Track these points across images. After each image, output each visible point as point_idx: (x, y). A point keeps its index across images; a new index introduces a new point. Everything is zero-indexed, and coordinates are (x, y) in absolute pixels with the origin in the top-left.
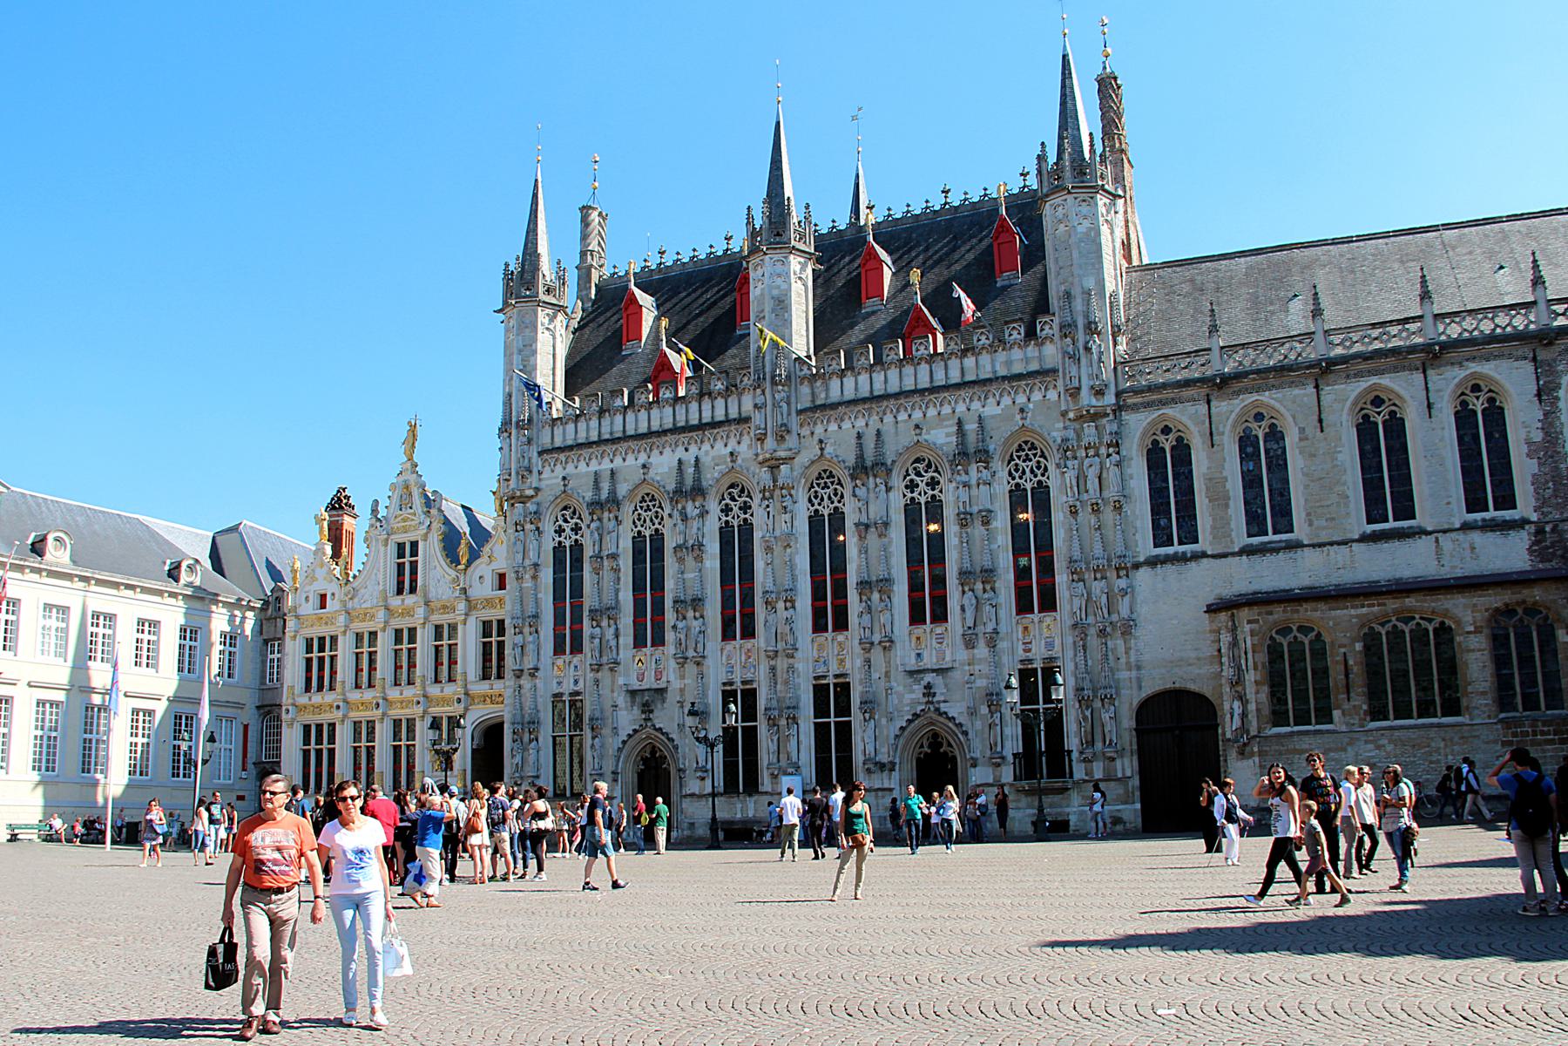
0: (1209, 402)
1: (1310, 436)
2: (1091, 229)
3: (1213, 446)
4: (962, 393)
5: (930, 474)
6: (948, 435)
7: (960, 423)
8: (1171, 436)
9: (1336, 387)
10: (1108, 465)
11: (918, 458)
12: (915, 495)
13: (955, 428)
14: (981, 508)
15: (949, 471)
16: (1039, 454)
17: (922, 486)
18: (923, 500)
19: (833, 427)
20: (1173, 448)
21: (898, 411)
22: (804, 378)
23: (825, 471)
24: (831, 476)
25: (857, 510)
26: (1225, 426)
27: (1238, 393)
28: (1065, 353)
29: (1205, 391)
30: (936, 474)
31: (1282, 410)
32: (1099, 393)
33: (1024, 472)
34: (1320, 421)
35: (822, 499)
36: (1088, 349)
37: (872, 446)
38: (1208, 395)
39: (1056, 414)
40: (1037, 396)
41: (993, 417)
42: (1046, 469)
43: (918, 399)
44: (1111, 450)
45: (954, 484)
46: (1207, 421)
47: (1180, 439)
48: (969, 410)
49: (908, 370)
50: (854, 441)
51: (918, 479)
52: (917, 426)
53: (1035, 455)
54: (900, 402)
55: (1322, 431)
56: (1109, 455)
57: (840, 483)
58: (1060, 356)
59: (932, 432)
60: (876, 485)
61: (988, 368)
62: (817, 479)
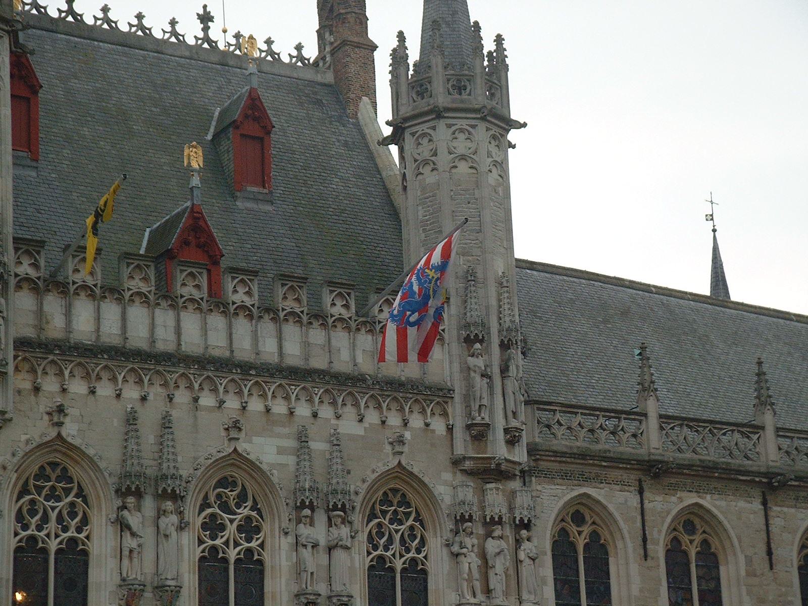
0: (641, 492)
1: (758, 573)
2: (499, 185)
3: (646, 556)
4: (308, 385)
5: (244, 511)
6: (281, 451)
7: (302, 438)
8: (586, 529)
9: (785, 509)
10: (522, 556)
11: (225, 478)
12: (218, 542)
13: (292, 443)
14: (337, 588)
15: (285, 516)
16: (413, 515)
17: (231, 529)
18: (232, 554)
19: (78, 387)
20: (586, 546)
21: (201, 389)
22: (28, 279)
23: (54, 465)
24: (65, 477)
25: (126, 552)
26: (660, 531)
27: (673, 488)
28: (467, 370)
29: (633, 477)
30: (254, 514)
31: (726, 523)
32: (512, 440)
33: (390, 541)
34: (770, 553)
35: (45, 519)
36: (504, 370)
37: (152, 439)
38: (640, 481)
39: (443, 457)
40: (416, 421)
41: (353, 438)
42: (423, 542)
43: (236, 377)
44: (524, 533)
45: (291, 539)
46: (639, 518)
47: (594, 536)
48: (315, 415)
49: (217, 321)
50: (116, 423)
51: (224, 515)
52: (236, 426)
53: (408, 514)
54: (206, 374)
55: (771, 568)
56: (518, 542)
57: (81, 494)
58: (456, 366)
59: (256, 440)
60: (161, 513)
61: (345, 355)
62: (37, 477)
